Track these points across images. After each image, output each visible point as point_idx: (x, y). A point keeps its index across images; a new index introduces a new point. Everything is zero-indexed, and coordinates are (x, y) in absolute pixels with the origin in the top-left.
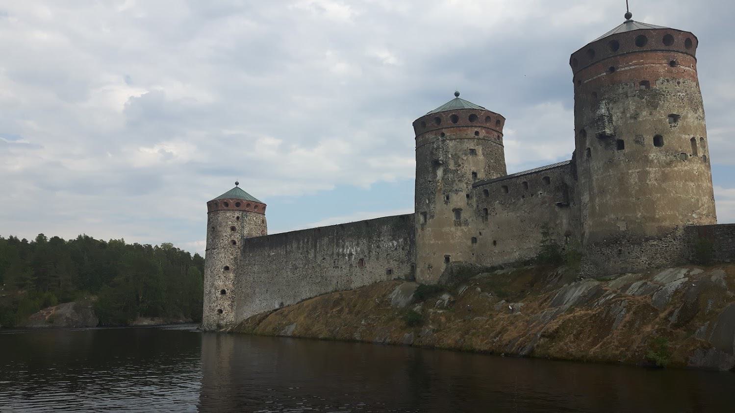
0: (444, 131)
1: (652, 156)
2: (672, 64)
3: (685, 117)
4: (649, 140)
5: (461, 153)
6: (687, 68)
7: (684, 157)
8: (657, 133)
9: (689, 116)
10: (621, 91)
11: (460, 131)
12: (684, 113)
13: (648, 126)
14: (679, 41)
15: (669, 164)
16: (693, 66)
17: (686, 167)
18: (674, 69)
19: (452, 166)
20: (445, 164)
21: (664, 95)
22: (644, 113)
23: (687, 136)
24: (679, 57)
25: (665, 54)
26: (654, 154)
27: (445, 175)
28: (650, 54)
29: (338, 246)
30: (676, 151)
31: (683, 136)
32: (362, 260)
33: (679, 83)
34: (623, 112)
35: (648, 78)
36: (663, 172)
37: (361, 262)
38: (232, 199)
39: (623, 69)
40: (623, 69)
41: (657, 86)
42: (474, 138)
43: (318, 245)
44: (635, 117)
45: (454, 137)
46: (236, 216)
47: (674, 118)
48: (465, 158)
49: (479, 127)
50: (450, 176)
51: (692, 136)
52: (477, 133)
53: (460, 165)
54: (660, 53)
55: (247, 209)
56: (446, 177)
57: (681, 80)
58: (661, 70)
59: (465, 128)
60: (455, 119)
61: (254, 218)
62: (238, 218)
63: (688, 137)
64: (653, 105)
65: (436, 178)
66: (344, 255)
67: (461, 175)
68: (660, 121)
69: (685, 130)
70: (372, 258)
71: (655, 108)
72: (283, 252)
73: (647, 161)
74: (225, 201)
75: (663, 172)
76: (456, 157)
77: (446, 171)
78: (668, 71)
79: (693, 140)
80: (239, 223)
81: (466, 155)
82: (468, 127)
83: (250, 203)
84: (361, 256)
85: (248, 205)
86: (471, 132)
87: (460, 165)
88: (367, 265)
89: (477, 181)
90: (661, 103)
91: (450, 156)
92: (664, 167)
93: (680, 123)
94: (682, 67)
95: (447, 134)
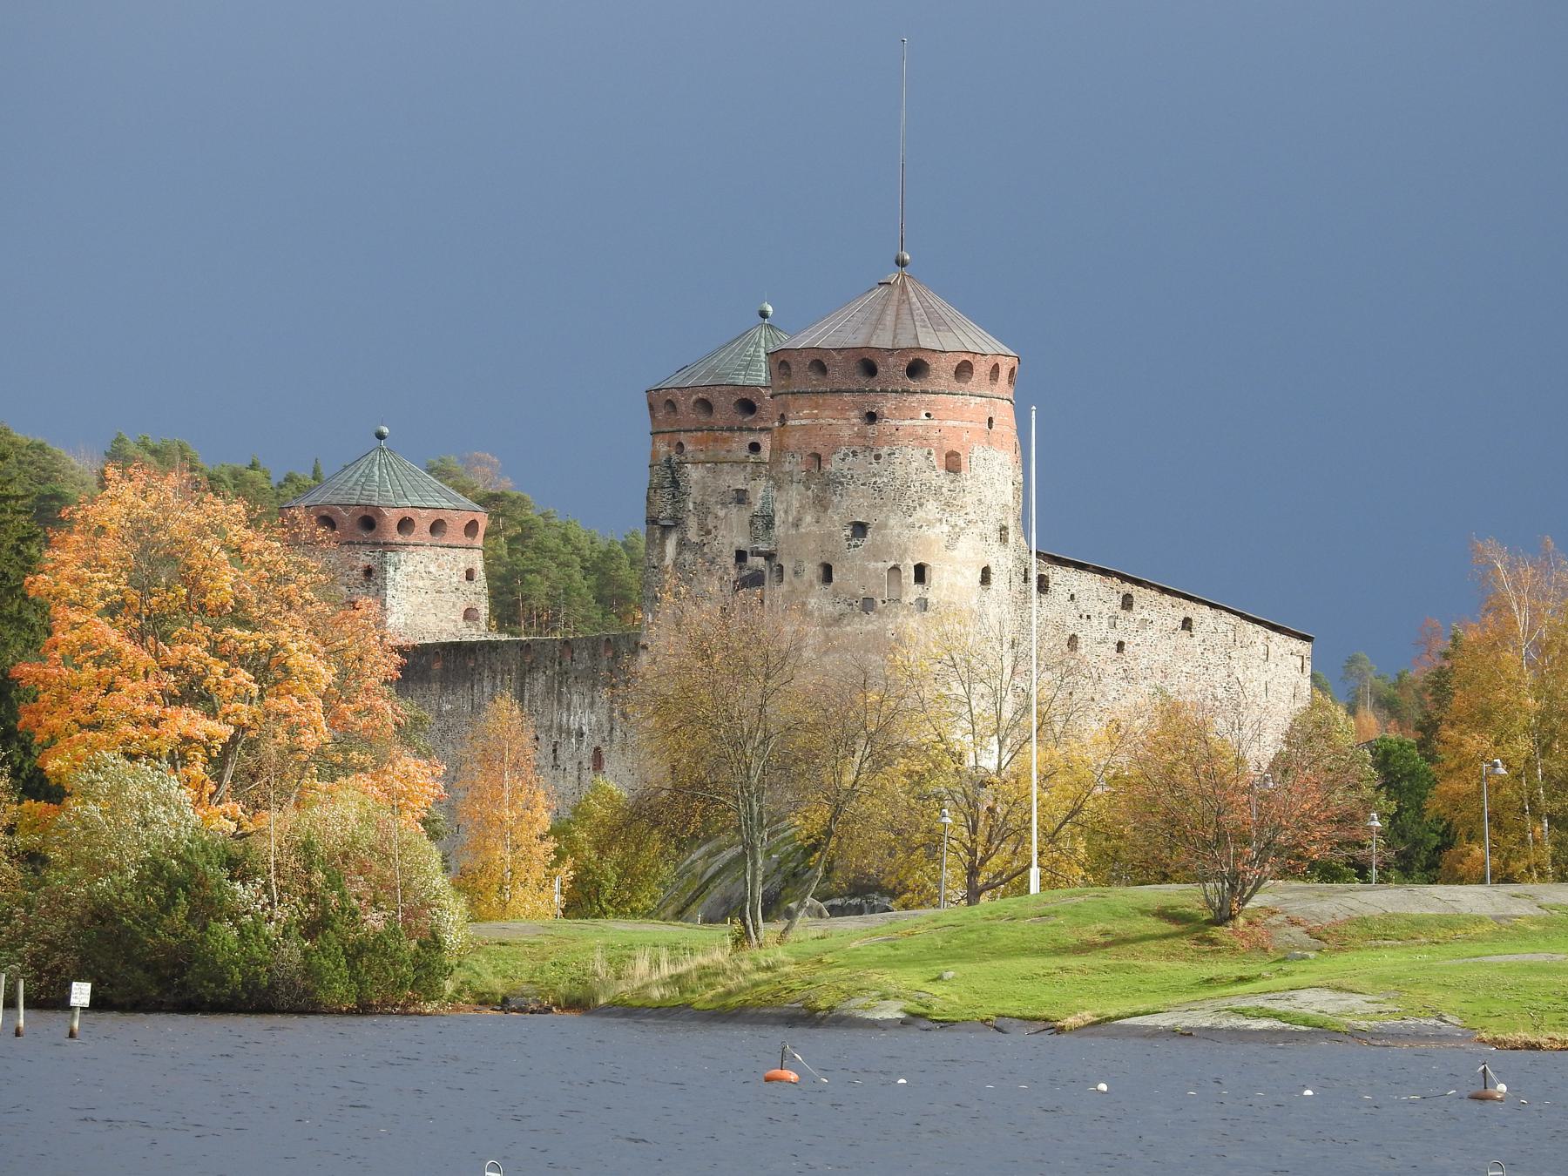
0: (683, 437)
1: (812, 602)
2: (872, 417)
3: (883, 526)
4: (811, 571)
5: (713, 500)
6: (907, 422)
7: (868, 605)
8: (825, 560)
9: (892, 522)
10: (787, 467)
11: (716, 440)
12: (881, 517)
13: (812, 546)
14: (893, 369)
15: (838, 620)
16: (928, 415)
17: (870, 627)
18: (870, 429)
19: (693, 535)
20: (677, 523)
21: (841, 483)
22: (808, 519)
23: (880, 565)
24: (887, 405)
25: (859, 398)
26: (819, 601)
27: (679, 554)
28: (828, 397)
29: (559, 701)
30: (854, 596)
31: (872, 565)
32: (597, 749)
33: (878, 457)
34: (786, 512)
35: (821, 450)
36: (827, 635)
37: (598, 760)
38: (346, 506)
39: (797, 422)
40: (797, 422)
41: (833, 465)
42: (742, 463)
43: (527, 695)
44: (796, 525)
45: (702, 457)
46: (361, 564)
47: (860, 529)
48: (721, 513)
49: (762, 430)
50: (689, 556)
51: (892, 563)
52: (755, 447)
53: (708, 532)
54: (847, 397)
55: (399, 539)
56: (681, 559)
57: (885, 451)
58: (846, 433)
59: (727, 434)
60: (706, 405)
61: (432, 568)
62: (368, 572)
63: (882, 566)
64: (821, 504)
65: (663, 560)
66: (569, 733)
67: (710, 556)
68: (830, 535)
69: (876, 554)
70: (616, 747)
71: (826, 509)
72: (467, 708)
73: (806, 613)
74: (325, 512)
75: (827, 635)
76: (703, 509)
77: (682, 545)
78: (858, 435)
79: (896, 568)
80: (373, 588)
81: (724, 504)
82: (730, 430)
83: (409, 513)
84: (597, 742)
85: (405, 525)
86: (738, 445)
87: (708, 532)
88: (606, 766)
89: (746, 573)
90: (836, 499)
91: (691, 506)
92: (829, 625)
93: (869, 535)
94: (893, 422)
95: (689, 448)
